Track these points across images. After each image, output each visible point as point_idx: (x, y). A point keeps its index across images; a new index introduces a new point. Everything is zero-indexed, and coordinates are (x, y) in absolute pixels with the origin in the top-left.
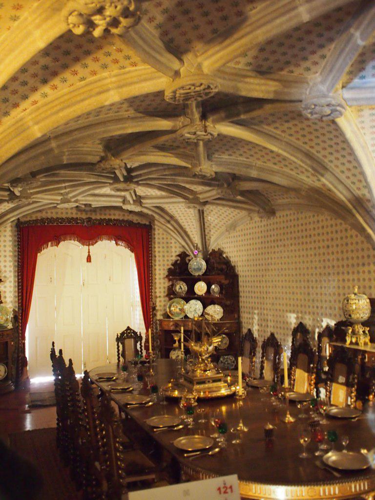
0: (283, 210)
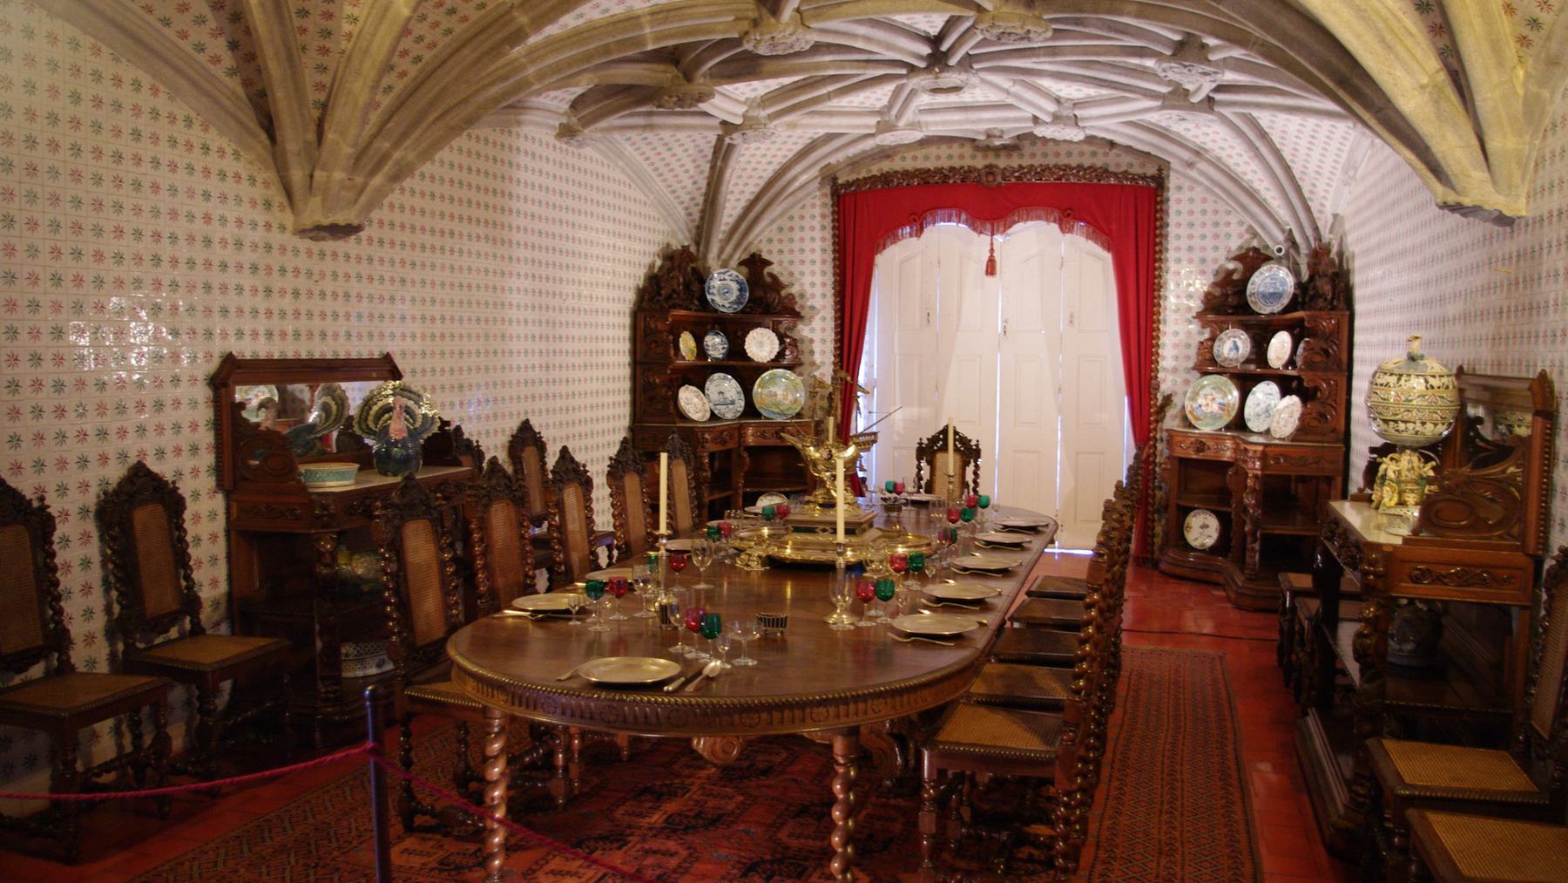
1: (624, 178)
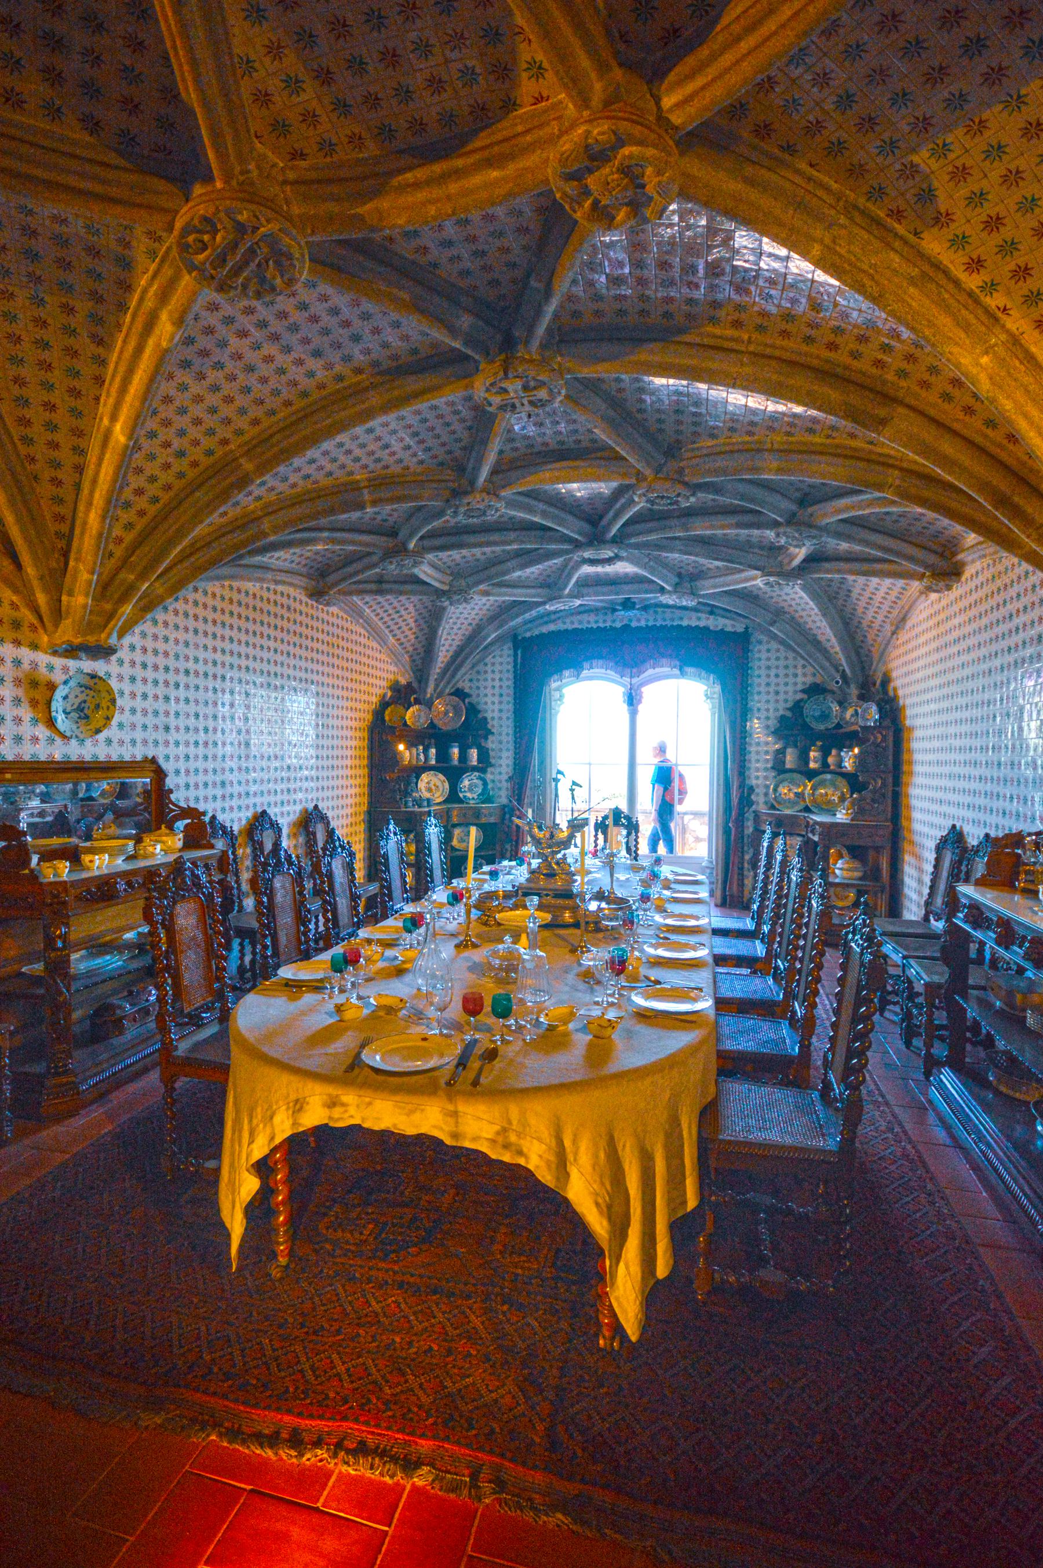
0: (973, 561)
1: (363, 631)
